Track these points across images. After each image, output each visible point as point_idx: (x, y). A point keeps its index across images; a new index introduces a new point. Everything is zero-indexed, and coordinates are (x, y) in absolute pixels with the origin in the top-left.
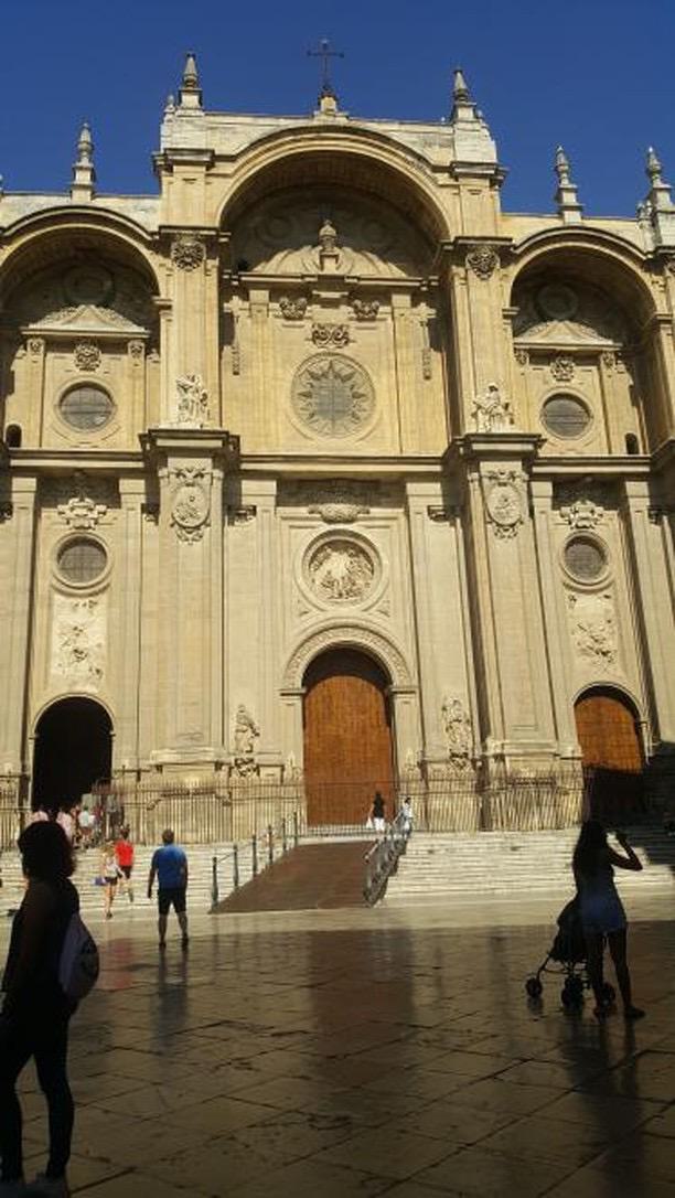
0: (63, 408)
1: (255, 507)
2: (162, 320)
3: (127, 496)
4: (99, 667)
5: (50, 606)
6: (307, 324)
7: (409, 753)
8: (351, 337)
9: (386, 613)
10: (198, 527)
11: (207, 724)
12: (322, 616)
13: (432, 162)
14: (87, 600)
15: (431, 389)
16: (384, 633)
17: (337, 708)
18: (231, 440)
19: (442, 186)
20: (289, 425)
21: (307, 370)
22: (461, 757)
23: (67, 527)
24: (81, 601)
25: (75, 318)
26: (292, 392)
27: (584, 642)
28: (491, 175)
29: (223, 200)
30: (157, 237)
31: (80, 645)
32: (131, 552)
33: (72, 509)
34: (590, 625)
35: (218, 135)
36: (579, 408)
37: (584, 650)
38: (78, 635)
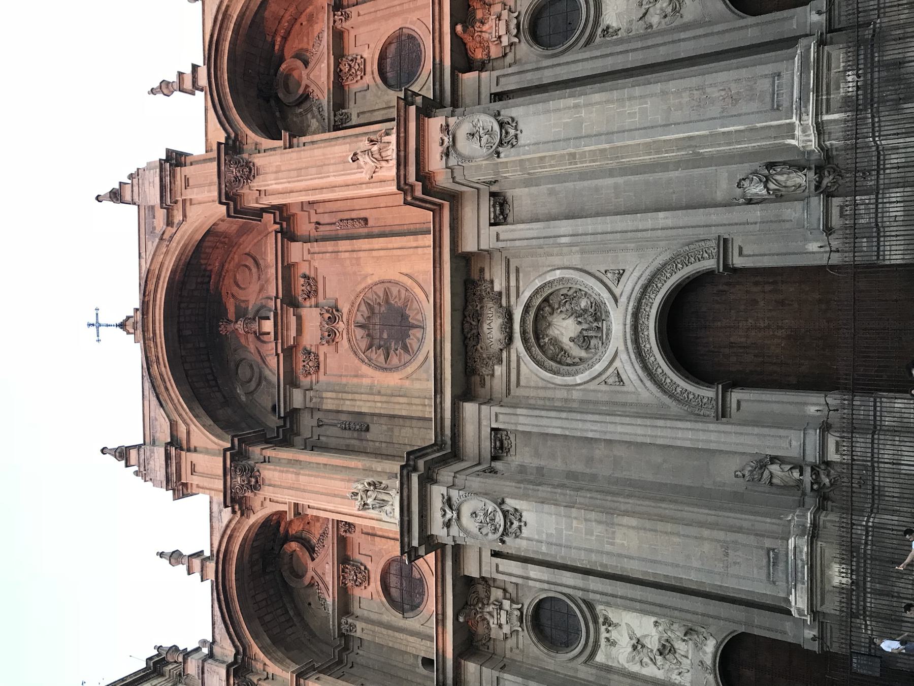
0: (406, 607)
1: (492, 429)
2: (309, 512)
3: (484, 569)
4: (683, 630)
5: (608, 669)
6: (323, 350)
7: (813, 247)
8: (332, 303)
9: (620, 274)
10: (505, 514)
11: (751, 540)
12: (623, 356)
13: (165, 227)
14: (603, 628)
15: (378, 219)
16: (643, 281)
17: (747, 337)
18: (412, 463)
19: (185, 216)
20: (414, 376)
21: (364, 353)
22: (821, 178)
23: (521, 634)
24: (604, 635)
25: (324, 583)
26: (384, 369)
27: (662, 9)
28: (171, 165)
29: (208, 438)
30: (237, 507)
31: (653, 644)
32: (545, 577)
33: (500, 626)
34: (641, 5)
35: (158, 435)
36: (393, 47)
37: (674, 9)
38: (643, 646)
